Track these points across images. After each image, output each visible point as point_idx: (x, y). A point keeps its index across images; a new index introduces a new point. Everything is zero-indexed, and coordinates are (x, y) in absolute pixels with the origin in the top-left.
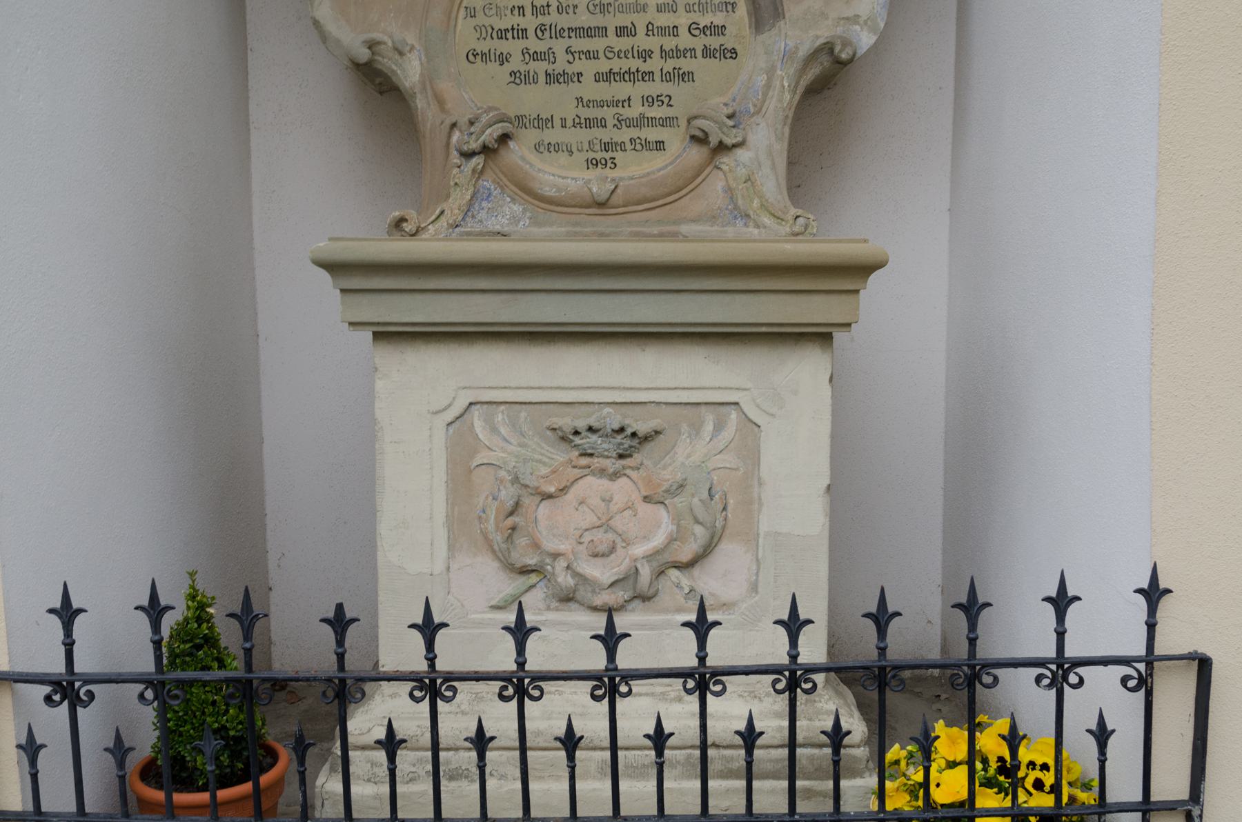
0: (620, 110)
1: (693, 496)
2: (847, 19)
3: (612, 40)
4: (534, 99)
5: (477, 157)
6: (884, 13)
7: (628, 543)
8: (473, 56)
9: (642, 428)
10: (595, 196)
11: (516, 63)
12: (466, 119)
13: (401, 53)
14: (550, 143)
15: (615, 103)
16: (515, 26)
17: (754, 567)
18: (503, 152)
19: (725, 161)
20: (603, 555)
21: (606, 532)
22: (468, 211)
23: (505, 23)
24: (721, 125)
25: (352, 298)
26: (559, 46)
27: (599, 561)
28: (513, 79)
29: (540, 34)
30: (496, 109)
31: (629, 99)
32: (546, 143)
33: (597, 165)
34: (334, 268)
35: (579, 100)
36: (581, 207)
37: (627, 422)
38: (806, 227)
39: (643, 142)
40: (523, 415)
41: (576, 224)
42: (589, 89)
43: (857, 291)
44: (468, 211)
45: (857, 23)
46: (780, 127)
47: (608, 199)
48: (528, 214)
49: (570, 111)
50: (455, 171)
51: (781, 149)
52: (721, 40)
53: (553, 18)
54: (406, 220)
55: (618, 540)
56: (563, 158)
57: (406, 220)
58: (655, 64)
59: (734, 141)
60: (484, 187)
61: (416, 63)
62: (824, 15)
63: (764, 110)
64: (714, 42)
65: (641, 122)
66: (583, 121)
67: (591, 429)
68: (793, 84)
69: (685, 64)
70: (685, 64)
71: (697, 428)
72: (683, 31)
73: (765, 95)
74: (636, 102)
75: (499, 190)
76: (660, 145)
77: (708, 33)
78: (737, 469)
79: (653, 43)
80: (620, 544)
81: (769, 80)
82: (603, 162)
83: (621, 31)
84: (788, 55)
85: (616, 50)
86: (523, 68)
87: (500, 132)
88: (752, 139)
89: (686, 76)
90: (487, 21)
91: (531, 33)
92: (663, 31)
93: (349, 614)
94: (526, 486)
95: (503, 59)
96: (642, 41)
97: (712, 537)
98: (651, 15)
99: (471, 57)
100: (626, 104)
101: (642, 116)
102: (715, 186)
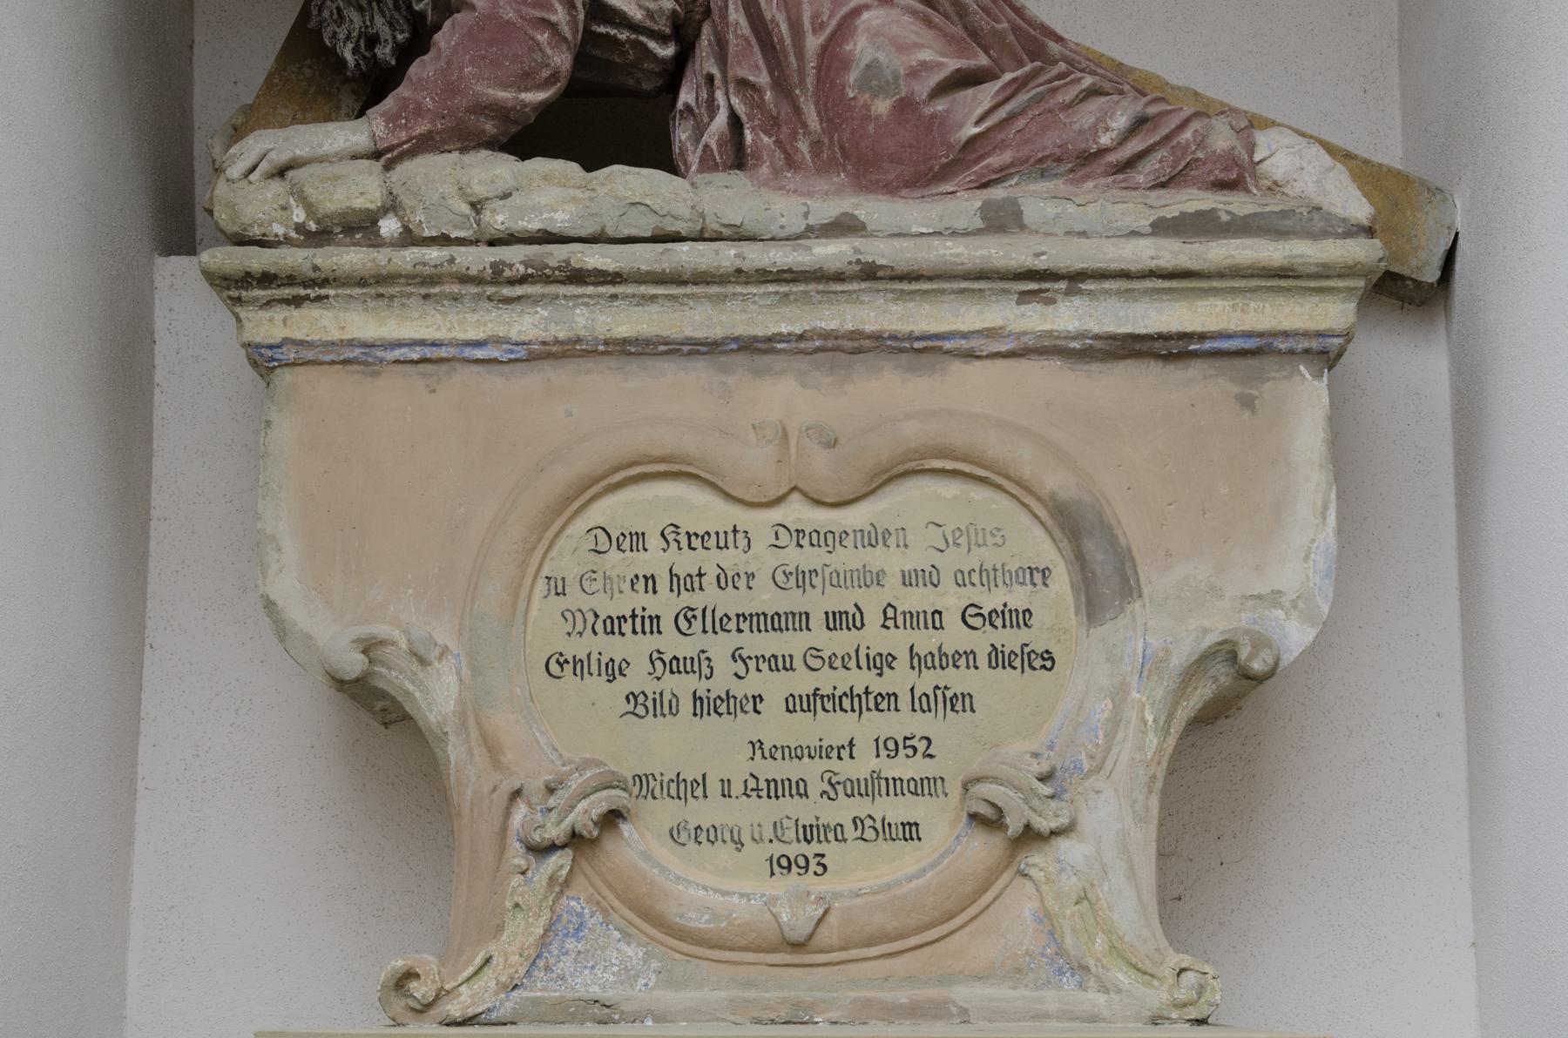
0: (834, 764)
2: (1260, 597)
3: (819, 636)
5: (559, 853)
8: (557, 664)
10: (786, 929)
11: (638, 679)
12: (539, 783)
13: (423, 662)
14: (699, 827)
15: (824, 752)
16: (639, 612)
18: (609, 844)
19: (1037, 860)
22: (537, 958)
23: (621, 606)
24: (1028, 795)
26: (720, 647)
28: (630, 707)
29: (683, 624)
30: (599, 764)
31: (851, 744)
32: (692, 827)
33: (789, 868)
35: (757, 745)
38: (1201, 990)
39: (879, 825)
41: (749, 984)
42: (776, 726)
44: (537, 958)
45: (1277, 604)
46: (1141, 798)
47: (811, 935)
48: (655, 965)
49: (738, 766)
50: (516, 880)
51: (1144, 840)
52: (1023, 635)
53: (710, 596)
54: (417, 976)
57: (417, 976)
58: (899, 680)
59: (1054, 825)
60: (570, 911)
61: (451, 679)
63: (1109, 765)
64: (1010, 639)
65: (874, 786)
66: (763, 785)
68: (1163, 718)
69: (957, 680)
70: (957, 680)
72: (952, 620)
73: (1110, 736)
74: (864, 749)
75: (599, 917)
76: (910, 831)
77: (999, 622)
79: (896, 641)
81: (1117, 710)
82: (802, 862)
83: (835, 621)
84: (1151, 665)
85: (826, 655)
86: (651, 687)
87: (604, 807)
88: (1086, 819)
89: (958, 702)
90: (586, 603)
91: (667, 624)
92: (914, 620)
95: (614, 670)
96: (875, 638)
98: (892, 591)
99: (554, 668)
100: (845, 754)
101: (876, 775)
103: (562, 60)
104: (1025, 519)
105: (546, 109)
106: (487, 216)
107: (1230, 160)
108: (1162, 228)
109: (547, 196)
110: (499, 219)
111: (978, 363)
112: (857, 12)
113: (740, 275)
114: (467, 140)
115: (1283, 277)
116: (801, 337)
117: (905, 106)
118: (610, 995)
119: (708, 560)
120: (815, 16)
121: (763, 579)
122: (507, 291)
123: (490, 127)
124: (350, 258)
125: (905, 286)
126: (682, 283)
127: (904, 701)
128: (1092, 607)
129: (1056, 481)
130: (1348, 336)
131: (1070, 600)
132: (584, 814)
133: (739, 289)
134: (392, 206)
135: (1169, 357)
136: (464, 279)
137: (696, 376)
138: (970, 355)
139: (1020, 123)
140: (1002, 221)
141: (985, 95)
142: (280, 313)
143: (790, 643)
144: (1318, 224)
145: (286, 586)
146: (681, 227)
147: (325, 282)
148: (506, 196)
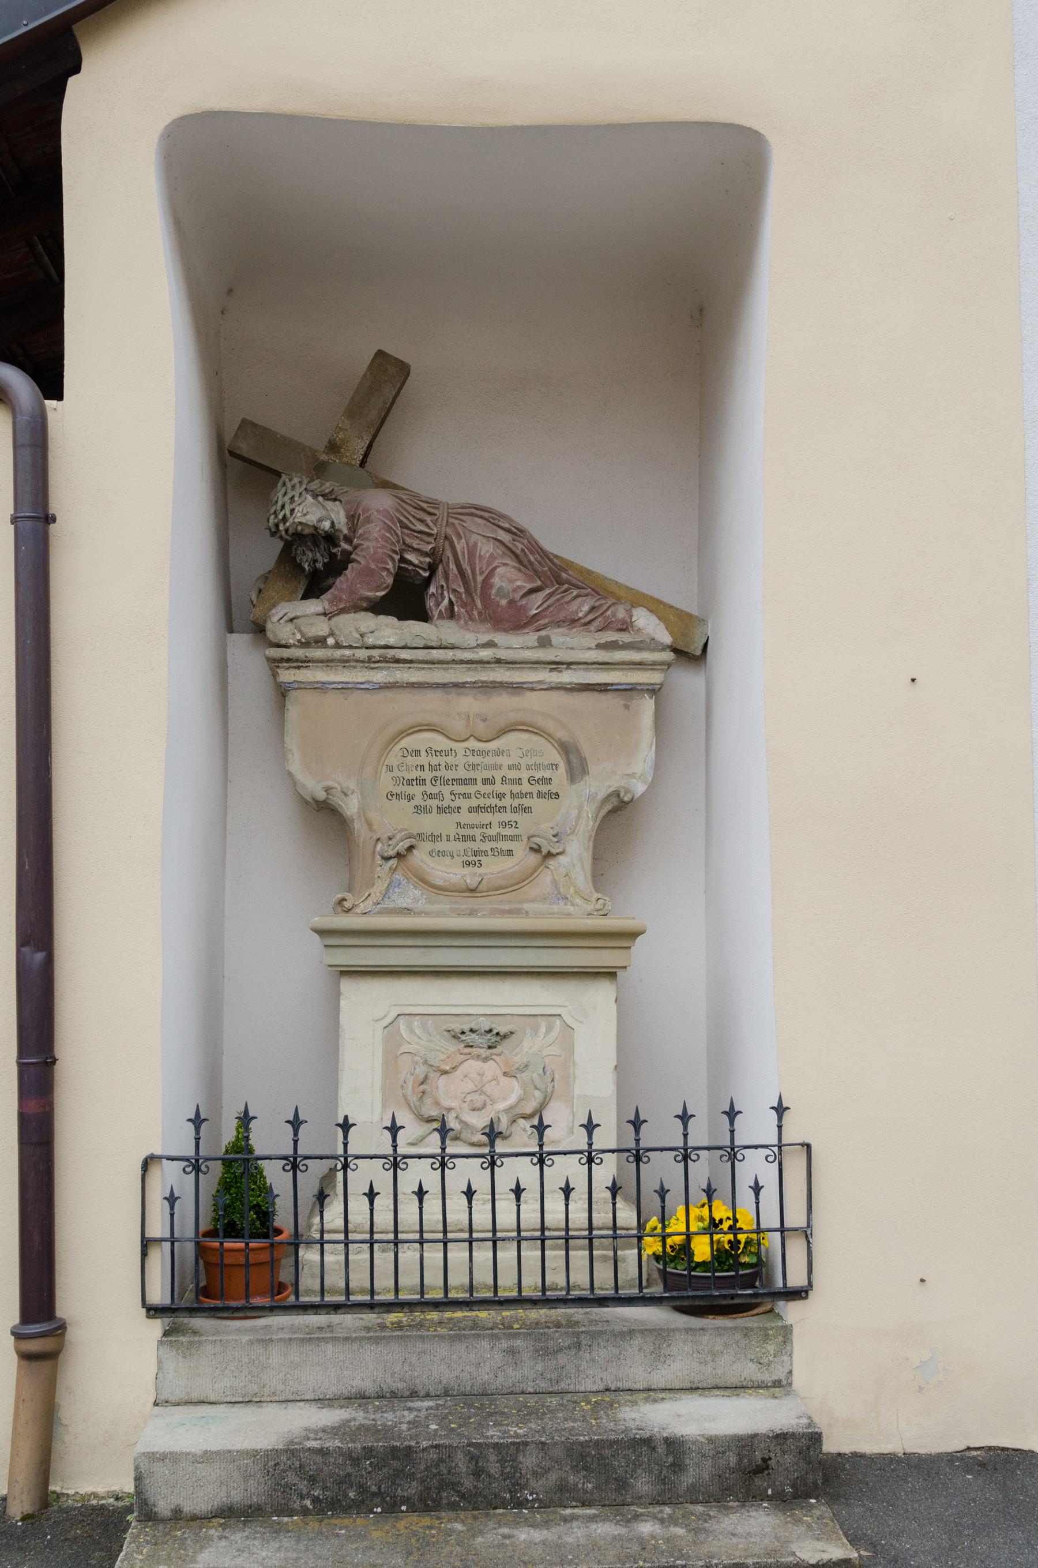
0: (484, 830)
1: (533, 1072)
2: (629, 775)
3: (480, 786)
4: (429, 823)
5: (393, 860)
6: (652, 772)
7: (493, 1102)
8: (390, 796)
9: (503, 1030)
10: (469, 885)
11: (418, 801)
12: (386, 836)
13: (346, 795)
14: (439, 851)
15: (481, 826)
16: (418, 778)
17: (571, 1118)
18: (410, 857)
19: (552, 863)
20: (478, 1110)
21: (480, 1095)
22: (385, 894)
23: (412, 775)
24: (549, 841)
25: (330, 951)
26: (446, 790)
27: (476, 1113)
28: (416, 810)
29: (434, 782)
30: (406, 830)
31: (490, 824)
32: (437, 851)
33: (469, 865)
34: (322, 933)
36: (459, 892)
37: (494, 1026)
38: (604, 905)
39: (499, 851)
40: (430, 1022)
41: (456, 903)
42: (465, 817)
43: (629, 948)
44: (385, 894)
45: (635, 778)
46: (586, 842)
47: (477, 888)
48: (425, 897)
49: (452, 831)
50: (379, 869)
51: (588, 857)
52: (549, 787)
53: (442, 773)
54: (346, 900)
55: (488, 1100)
56: (447, 860)
57: (346, 900)
58: (507, 802)
59: (558, 851)
60: (396, 879)
61: (355, 801)
62: (614, 773)
63: (576, 831)
64: (544, 788)
66: (461, 837)
67: (472, 1030)
68: (595, 816)
69: (526, 802)
70: (526, 802)
71: (535, 1030)
72: (525, 782)
73: (577, 822)
74: (495, 825)
75: (406, 881)
76: (510, 852)
77: (541, 783)
78: (560, 1056)
79: (506, 789)
80: (489, 1102)
81: (580, 812)
82: (473, 863)
83: (486, 781)
84: (591, 798)
85: (482, 793)
86: (423, 804)
87: (409, 844)
88: (568, 849)
89: (527, 810)
90: (400, 774)
91: (428, 782)
92: (512, 781)
93: (351, 1122)
94: (432, 1066)
95: (410, 798)
96: (499, 788)
97: (545, 1098)
98: (505, 771)
99: (389, 796)
100: (488, 827)
101: (499, 834)
102: (545, 879)
103: (390, 581)
104: (550, 747)
105: (383, 597)
106: (366, 639)
107: (623, 621)
108: (599, 646)
109: (387, 632)
110: (370, 640)
111: (535, 692)
112: (495, 568)
113: (454, 662)
114: (356, 608)
115: (640, 665)
116: (474, 683)
117: (512, 602)
118: (410, 906)
119: (442, 760)
120: (481, 569)
121: (461, 767)
122: (372, 665)
123: (365, 605)
124: (319, 653)
125: (511, 666)
126: (433, 663)
127: (508, 809)
128: (572, 778)
129: (561, 734)
130: (662, 685)
131: (565, 775)
132: (402, 846)
133: (453, 666)
134: (332, 634)
135: (601, 691)
136: (358, 661)
137: (439, 694)
138: (533, 689)
139: (551, 609)
140: (544, 643)
141: (540, 596)
142: (292, 671)
143: (470, 789)
144: (653, 645)
145: (295, 766)
146: (433, 644)
147: (309, 661)
148: (372, 632)
